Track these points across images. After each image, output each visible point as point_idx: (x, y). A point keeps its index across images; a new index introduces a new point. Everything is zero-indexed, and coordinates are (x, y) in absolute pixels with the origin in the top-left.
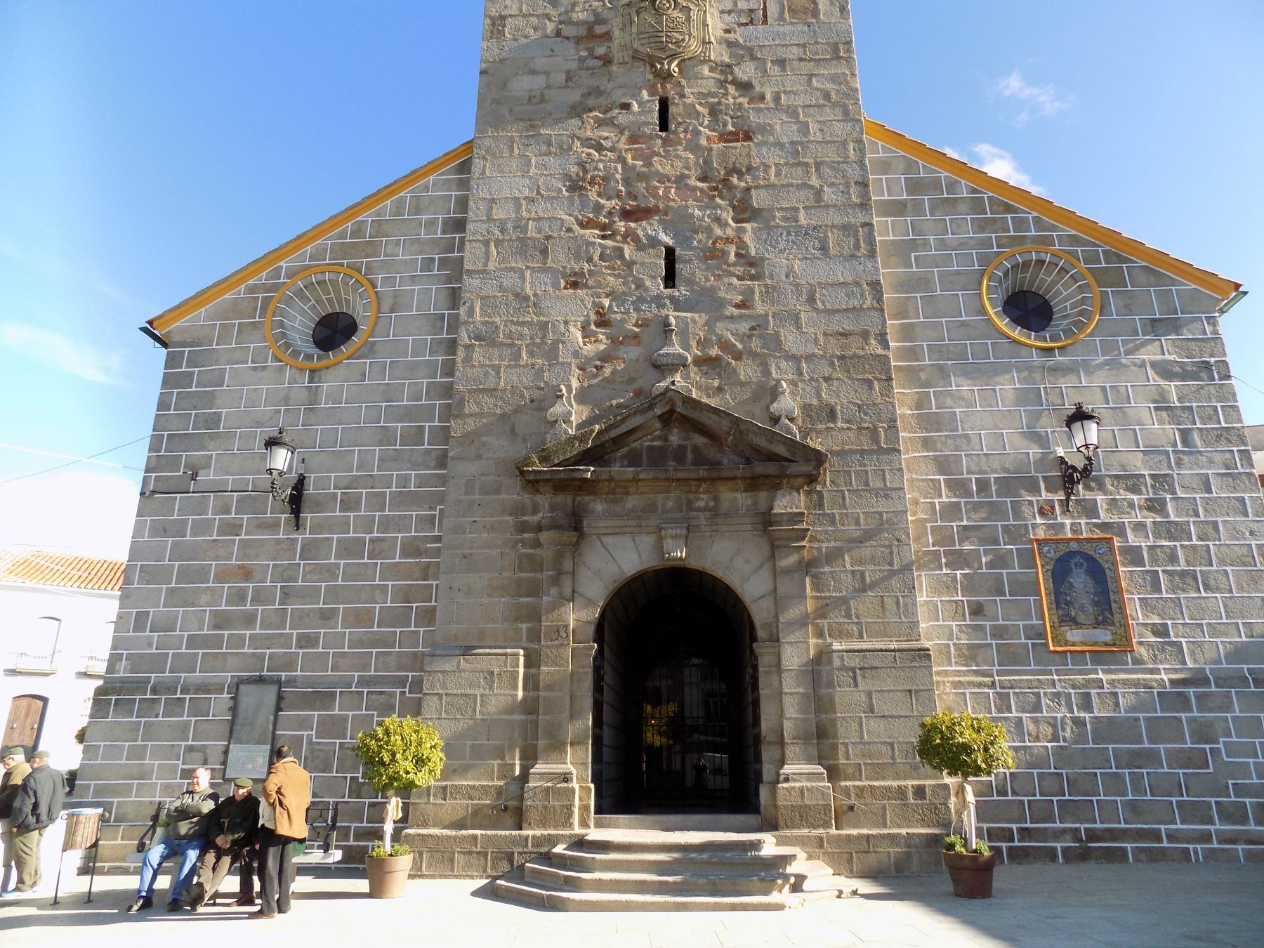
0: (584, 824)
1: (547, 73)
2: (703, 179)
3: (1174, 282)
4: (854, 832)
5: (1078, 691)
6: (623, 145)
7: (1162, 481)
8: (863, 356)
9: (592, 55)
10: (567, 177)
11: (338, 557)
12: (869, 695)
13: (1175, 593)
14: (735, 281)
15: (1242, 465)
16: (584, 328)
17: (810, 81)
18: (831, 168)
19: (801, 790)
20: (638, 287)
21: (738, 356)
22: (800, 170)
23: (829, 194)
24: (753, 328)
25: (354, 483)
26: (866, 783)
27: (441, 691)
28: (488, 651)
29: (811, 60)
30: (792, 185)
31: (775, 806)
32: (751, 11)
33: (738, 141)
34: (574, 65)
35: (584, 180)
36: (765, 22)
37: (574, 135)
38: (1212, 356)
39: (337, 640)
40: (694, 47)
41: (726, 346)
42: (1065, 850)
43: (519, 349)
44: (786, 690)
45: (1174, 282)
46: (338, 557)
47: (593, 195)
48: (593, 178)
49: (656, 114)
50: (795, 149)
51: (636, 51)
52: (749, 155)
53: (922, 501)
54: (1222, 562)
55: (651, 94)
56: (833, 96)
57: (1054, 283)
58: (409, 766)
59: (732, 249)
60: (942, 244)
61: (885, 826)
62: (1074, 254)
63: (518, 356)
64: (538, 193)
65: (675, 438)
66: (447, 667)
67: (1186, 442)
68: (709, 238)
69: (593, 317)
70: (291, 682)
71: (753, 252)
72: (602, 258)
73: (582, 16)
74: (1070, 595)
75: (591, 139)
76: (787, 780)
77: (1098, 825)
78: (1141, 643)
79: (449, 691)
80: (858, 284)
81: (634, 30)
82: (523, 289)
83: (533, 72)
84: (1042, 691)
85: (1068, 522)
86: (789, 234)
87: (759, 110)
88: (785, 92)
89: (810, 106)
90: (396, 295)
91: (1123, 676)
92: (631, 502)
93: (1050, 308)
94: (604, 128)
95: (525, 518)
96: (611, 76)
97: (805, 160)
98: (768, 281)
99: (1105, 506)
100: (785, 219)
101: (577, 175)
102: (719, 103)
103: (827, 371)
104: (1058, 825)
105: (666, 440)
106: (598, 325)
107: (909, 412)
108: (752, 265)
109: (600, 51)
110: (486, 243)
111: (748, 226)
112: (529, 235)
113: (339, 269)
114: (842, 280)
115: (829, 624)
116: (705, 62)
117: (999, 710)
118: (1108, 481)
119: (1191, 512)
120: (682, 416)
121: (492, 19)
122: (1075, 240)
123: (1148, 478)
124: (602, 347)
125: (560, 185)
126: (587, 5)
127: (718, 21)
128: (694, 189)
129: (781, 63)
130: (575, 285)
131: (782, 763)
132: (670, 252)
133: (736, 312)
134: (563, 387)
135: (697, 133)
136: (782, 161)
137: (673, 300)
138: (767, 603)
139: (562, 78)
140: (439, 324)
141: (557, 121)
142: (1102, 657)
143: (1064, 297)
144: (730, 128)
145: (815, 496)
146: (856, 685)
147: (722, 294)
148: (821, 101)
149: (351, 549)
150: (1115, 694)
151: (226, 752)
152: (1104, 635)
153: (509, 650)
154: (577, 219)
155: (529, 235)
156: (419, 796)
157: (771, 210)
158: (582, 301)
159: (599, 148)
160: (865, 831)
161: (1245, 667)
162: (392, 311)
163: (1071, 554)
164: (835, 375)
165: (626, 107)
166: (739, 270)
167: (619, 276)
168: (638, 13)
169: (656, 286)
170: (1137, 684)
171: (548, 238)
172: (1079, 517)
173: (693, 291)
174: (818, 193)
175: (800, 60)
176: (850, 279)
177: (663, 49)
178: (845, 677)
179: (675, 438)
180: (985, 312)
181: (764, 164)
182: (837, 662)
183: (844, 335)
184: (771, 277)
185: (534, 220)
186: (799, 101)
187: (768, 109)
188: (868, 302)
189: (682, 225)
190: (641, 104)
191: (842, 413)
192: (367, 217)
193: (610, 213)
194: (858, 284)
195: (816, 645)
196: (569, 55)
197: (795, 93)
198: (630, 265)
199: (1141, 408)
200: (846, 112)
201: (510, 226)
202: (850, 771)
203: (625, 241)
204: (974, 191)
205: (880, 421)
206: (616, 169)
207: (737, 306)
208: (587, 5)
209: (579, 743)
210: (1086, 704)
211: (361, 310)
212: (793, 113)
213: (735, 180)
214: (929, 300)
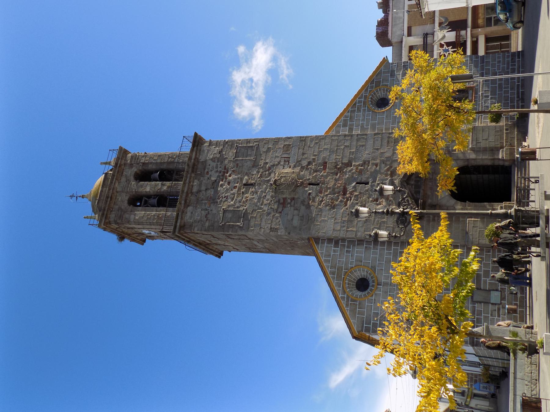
0: (514, 204)
1: (293, 215)
2: (337, 175)
3: (381, 70)
4: (516, 143)
6: (322, 195)
9: (290, 203)
10: (330, 210)
12: (483, 140)
14: (369, 167)
16: (378, 205)
17: (311, 147)
18: (339, 143)
19: (505, 154)
20: (367, 191)
21: (391, 167)
22: (339, 151)
23: (347, 144)
24: (384, 163)
26: (504, 141)
27: (478, 239)
28: (467, 228)
29: (304, 147)
30: (343, 153)
31: (510, 160)
32: (285, 161)
33: (326, 165)
34: (292, 208)
35: (331, 205)
36: (289, 158)
37: (316, 208)
38: (402, 64)
41: (388, 170)
42: (521, 103)
43: (382, 221)
44: (481, 158)
45: (381, 70)
47: (337, 203)
48: (331, 203)
49: (314, 186)
50: (331, 152)
51: (292, 191)
52: (331, 163)
57: (377, 96)
60: (363, 120)
61: (515, 137)
62: (370, 91)
63: (384, 222)
64: (333, 217)
65: (413, 182)
66: (471, 238)
68: (355, 173)
69: (375, 202)
71: (361, 163)
72: (357, 200)
73: (276, 206)
75: (319, 203)
76: (503, 157)
77: (516, 96)
78: (473, 85)
80: (374, 138)
81: (285, 191)
82: (364, 221)
83: (292, 219)
86: (357, 154)
88: (313, 153)
89: (319, 147)
90: (356, 261)
91: (481, 89)
92: (429, 193)
93: (382, 98)
94: (315, 200)
95: (431, 219)
96: (299, 198)
97: (336, 149)
98: (371, 159)
100: (353, 155)
102: (313, 170)
104: (516, 104)
105: (412, 185)
106: (377, 201)
108: (365, 163)
109: (289, 201)
110: (347, 231)
111: (353, 164)
112: (347, 219)
113: (345, 278)
114: (373, 142)
116: (299, 173)
120: (407, 179)
122: (366, 90)
124: (384, 200)
125: (332, 211)
126: (272, 205)
127: (286, 170)
128: (340, 176)
129: (303, 154)
131: (499, 159)
133: (378, 167)
135: (322, 176)
136: (335, 155)
137: (372, 183)
138: (459, 162)
139: (296, 212)
140: (368, 248)
141: (311, 213)
142: (476, 93)
143: (380, 94)
144: (322, 167)
146: (481, 142)
147: (373, 170)
150: (485, 91)
151: (493, 304)
152: (470, 92)
153: (467, 222)
154: (344, 207)
155: (347, 219)
157: (349, 158)
158: (370, 205)
159: (322, 201)
160: (516, 140)
161: (479, 65)
162: (362, 261)
165: (310, 194)
166: (366, 166)
167: (363, 196)
168: (280, 190)
169: (368, 187)
170: (483, 86)
173: (370, 178)
174: (346, 146)
175: (303, 149)
176: (373, 140)
178: (478, 145)
179: (413, 182)
180: (384, 111)
181: (335, 159)
182: (474, 146)
183: (388, 142)
184: (369, 158)
185: (342, 218)
186: (317, 150)
187: (318, 158)
188: (380, 136)
189: (349, 181)
190: (309, 190)
192: (328, 271)
193: (344, 198)
194: (374, 138)
195: (470, 151)
196: (289, 210)
197: (314, 151)
198: (360, 193)
200: (323, 139)
201: (342, 225)
202: (501, 144)
203: (353, 194)
204: (348, 112)
206: (329, 197)
207: (377, 167)
208: (272, 205)
209: (493, 206)
210: (487, 97)
211: (358, 274)
212: (320, 152)
213: (339, 166)
214: (379, 124)
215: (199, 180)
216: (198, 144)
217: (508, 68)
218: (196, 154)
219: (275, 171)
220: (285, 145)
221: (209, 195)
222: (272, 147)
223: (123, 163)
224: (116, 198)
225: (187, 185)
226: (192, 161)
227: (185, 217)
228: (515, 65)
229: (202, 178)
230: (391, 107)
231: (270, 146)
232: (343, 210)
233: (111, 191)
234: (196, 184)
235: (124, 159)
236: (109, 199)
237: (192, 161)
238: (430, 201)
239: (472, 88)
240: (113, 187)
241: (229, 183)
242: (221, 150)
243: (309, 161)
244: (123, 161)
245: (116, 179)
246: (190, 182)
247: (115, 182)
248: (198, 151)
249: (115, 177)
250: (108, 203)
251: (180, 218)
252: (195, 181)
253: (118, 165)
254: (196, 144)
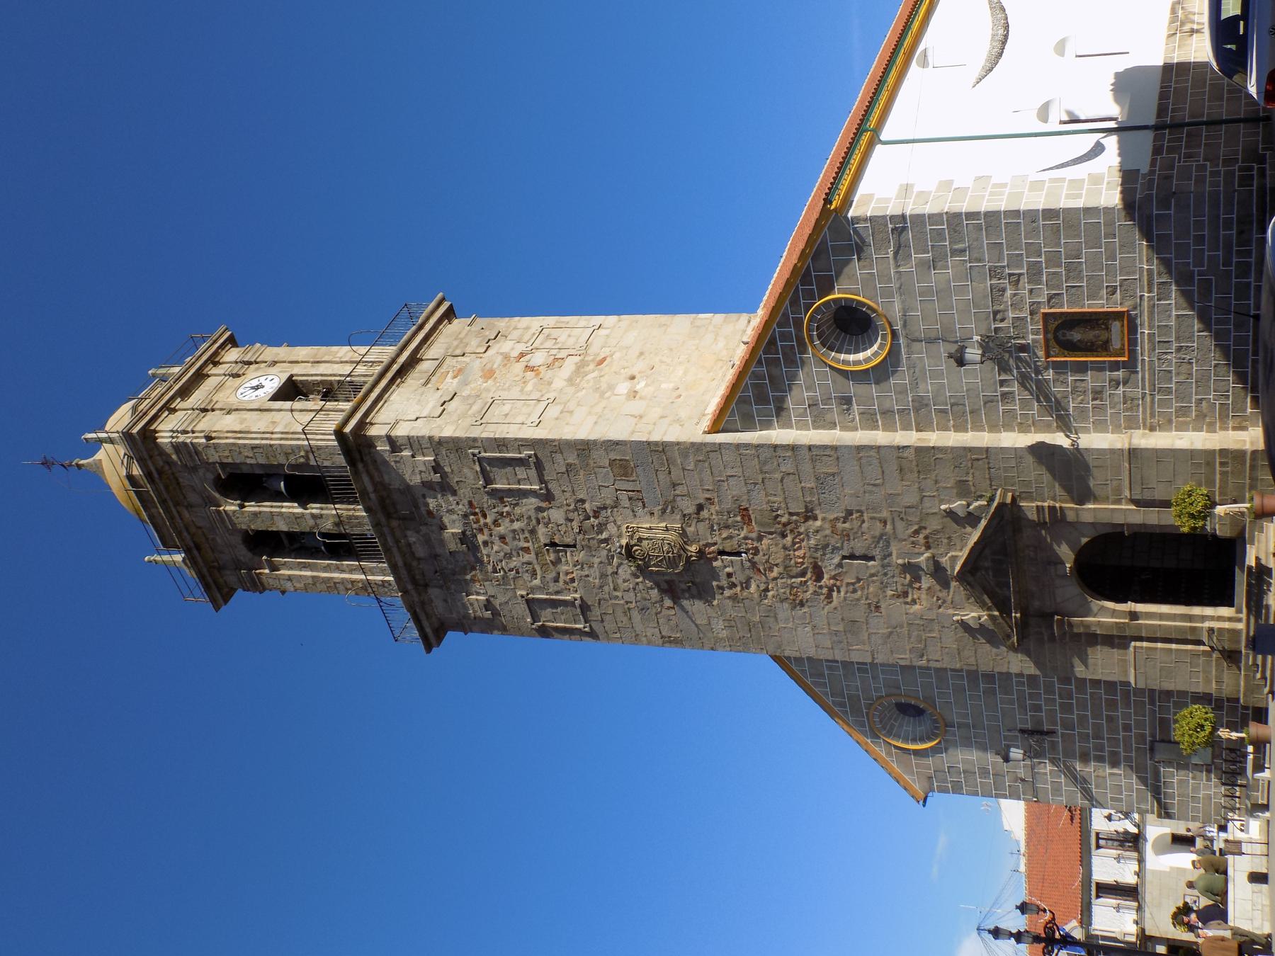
2: (784, 536)
3: (824, 242)
5: (1157, 347)
7: (994, 273)
8: (917, 462)
11: (1072, 714)
13: (1083, 278)
14: (865, 525)
15: (978, 220)
25: (1023, 707)
32: (630, 499)
35: (794, 600)
37: (758, 604)
39: (1127, 716)
40: (672, 537)
41: (916, 532)
45: (824, 242)
46: (1072, 714)
53: (1019, 421)
54: (1058, 245)
55: (716, 559)
56: (701, 458)
58: (1203, 734)
59: (840, 525)
67: (962, 251)
69: (901, 600)
70: (1153, 735)
74: (1087, 343)
79: (1158, 675)
84: (1157, 369)
85: (1031, 337)
87: (720, 501)
99: (1017, 312)
101: (791, 603)
103: (930, 482)
104: (1250, 370)
107: (952, 422)
115: (1113, 495)
117: (1170, 393)
118: (996, 308)
119: (1019, 258)
121: (664, 643)
123: (992, 282)
129: (674, 485)
130: (877, 607)
132: (844, 557)
133: (889, 527)
134: (955, 618)
142: (1133, 328)
144: (739, 518)
145: (1024, 495)
148: (706, 464)
149: (1067, 708)
152: (1116, 326)
156: (1221, 693)
163: (1056, 339)
164: (934, 478)
165: (729, 575)
167: (868, 585)
171: (843, 619)
172: (1027, 328)
177: (680, 556)
191: (961, 477)
192: (830, 701)
197: (701, 481)
199: (935, 278)
201: (835, 638)
203: (842, 581)
204: (760, 362)
205: (966, 456)
215: (418, 532)
216: (360, 452)
217: (1227, 263)
218: (371, 478)
219: (615, 522)
220: (612, 462)
221: (465, 563)
222: (576, 462)
223: (161, 463)
224: (207, 539)
225: (395, 550)
226: (373, 496)
227: (433, 609)
228: (1249, 253)
229: (424, 529)
230: (886, 357)
231: (570, 461)
232: (826, 610)
233: (185, 534)
234: (414, 539)
235: (156, 453)
236: (195, 552)
237: (373, 496)
238: (1037, 604)
239: (1118, 316)
240: (182, 525)
241: (502, 538)
242: (433, 464)
243: (698, 502)
244: (158, 458)
245: (175, 506)
246: (397, 542)
247: (178, 512)
248: (371, 467)
249: (171, 504)
250: (199, 560)
251: (423, 617)
252: (409, 533)
253: (156, 475)
254: (357, 456)
